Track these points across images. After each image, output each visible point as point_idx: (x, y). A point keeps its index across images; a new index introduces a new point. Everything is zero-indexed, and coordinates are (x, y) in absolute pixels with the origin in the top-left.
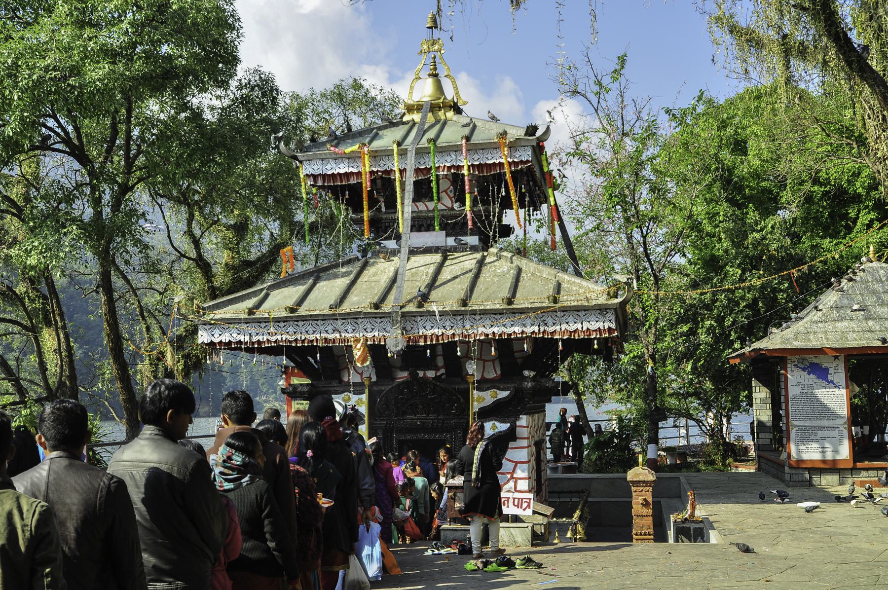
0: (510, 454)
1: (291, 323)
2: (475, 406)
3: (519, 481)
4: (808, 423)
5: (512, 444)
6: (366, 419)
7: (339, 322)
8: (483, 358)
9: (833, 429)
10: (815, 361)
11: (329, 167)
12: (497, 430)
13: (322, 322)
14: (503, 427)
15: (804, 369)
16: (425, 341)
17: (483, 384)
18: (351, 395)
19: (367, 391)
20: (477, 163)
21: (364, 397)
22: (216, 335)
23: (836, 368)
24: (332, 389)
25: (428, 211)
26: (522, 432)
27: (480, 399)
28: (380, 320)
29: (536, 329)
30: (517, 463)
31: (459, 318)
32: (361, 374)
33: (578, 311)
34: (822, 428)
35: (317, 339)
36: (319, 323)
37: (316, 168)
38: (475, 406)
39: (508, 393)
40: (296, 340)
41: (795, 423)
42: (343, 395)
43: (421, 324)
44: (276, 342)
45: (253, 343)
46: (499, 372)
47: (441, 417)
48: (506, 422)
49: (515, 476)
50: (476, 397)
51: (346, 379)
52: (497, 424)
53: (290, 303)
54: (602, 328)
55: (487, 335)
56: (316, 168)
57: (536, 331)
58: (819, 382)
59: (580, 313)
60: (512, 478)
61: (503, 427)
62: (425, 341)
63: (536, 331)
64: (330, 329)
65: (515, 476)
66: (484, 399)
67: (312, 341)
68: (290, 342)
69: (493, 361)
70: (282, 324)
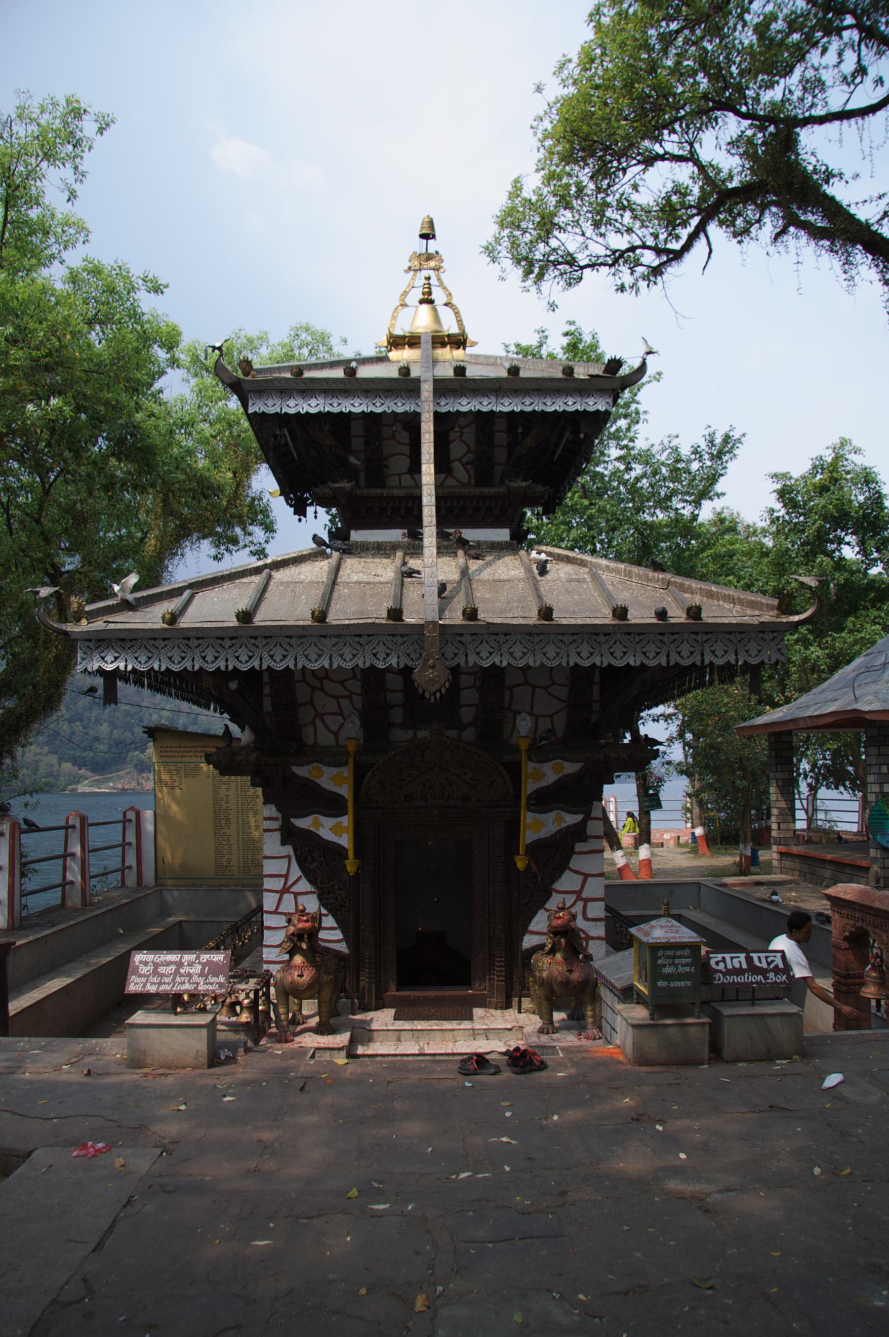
0: (576, 862)
2: (530, 786)
3: (590, 904)
5: (579, 847)
8: (535, 711)
11: (292, 403)
12: (564, 825)
17: (540, 751)
19: (351, 760)
21: (347, 772)
22: (109, 658)
30: (586, 876)
32: (336, 734)
33: (730, 633)
38: (530, 786)
39: (578, 766)
42: (310, 767)
49: (584, 895)
50: (530, 771)
51: (310, 741)
52: (563, 813)
53: (243, 604)
59: (732, 637)
60: (579, 898)
61: (571, 819)
65: (584, 895)
69: (551, 716)
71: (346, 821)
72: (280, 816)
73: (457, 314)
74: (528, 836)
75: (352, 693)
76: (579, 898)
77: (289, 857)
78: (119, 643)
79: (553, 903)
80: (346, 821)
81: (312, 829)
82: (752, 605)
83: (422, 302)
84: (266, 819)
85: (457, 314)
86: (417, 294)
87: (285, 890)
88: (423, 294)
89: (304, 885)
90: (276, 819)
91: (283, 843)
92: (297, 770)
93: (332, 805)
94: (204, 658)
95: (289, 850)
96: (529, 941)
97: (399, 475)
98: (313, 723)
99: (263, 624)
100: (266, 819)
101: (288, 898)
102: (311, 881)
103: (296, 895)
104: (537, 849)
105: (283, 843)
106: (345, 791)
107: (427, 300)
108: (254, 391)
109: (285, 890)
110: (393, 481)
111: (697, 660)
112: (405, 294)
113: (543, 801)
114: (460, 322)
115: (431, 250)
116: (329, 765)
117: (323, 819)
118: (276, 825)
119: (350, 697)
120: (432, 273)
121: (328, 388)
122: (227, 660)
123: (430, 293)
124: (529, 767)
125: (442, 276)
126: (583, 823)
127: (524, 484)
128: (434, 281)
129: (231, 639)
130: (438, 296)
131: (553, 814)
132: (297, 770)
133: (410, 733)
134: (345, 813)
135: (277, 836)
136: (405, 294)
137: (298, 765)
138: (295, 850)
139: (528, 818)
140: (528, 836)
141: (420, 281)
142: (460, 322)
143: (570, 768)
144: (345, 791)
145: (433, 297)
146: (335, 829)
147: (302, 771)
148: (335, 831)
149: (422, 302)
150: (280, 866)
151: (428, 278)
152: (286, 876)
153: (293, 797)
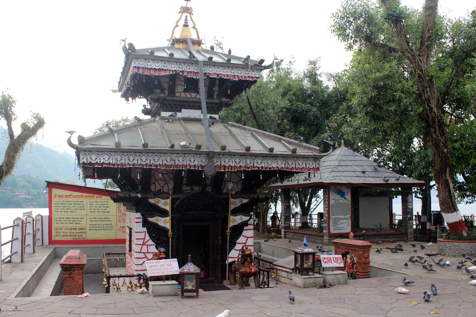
0: (244, 233)
1: (144, 154)
2: (232, 207)
4: (337, 217)
5: (246, 228)
6: (170, 213)
7: (175, 155)
9: (346, 219)
10: (340, 189)
11: (149, 64)
12: (243, 220)
13: (164, 155)
15: (336, 193)
16: (225, 169)
18: (160, 199)
19: (170, 197)
20: (233, 74)
21: (169, 201)
23: (348, 192)
24: (149, 196)
25: (192, 98)
27: (235, 203)
28: (199, 156)
29: (284, 166)
30: (248, 238)
31: (244, 157)
34: (341, 219)
35: (160, 164)
36: (162, 155)
37: (141, 63)
38: (232, 207)
40: (146, 165)
41: (332, 216)
42: (155, 199)
43: (222, 160)
44: (133, 165)
45: (118, 165)
46: (240, 189)
47: (210, 212)
48: (247, 216)
50: (232, 201)
52: (243, 217)
55: (259, 168)
56: (141, 63)
57: (284, 167)
58: (341, 198)
62: (225, 169)
63: (284, 167)
64: (169, 159)
66: (236, 203)
67: (156, 166)
68: (143, 165)
69: (237, 182)
70: (138, 154)
71: (168, 219)
72: (141, 217)
73: (197, 32)
74: (231, 224)
75: (168, 173)
76: (245, 245)
77: (145, 232)
78: (97, 153)
79: (238, 247)
80: (168, 219)
81: (156, 222)
82: (309, 148)
84: (136, 218)
85: (197, 32)
86: (182, 23)
87: (144, 244)
88: (185, 23)
89: (151, 242)
90: (140, 218)
91: (143, 226)
92: (150, 200)
93: (164, 213)
94: (129, 159)
95: (145, 229)
96: (230, 260)
97: (180, 93)
98: (155, 183)
99: (152, 148)
100: (136, 218)
101: (145, 247)
102: (153, 241)
103: (147, 245)
104: (234, 228)
105: (143, 226)
106: (168, 208)
107: (186, 25)
108: (136, 58)
109: (144, 244)
110: (177, 95)
111: (294, 166)
112: (178, 21)
113: (236, 212)
114: (198, 35)
115: (189, 6)
116: (162, 199)
117: (159, 218)
118: (141, 220)
119: (168, 174)
120: (188, 15)
121: (162, 59)
122: (138, 160)
123: (187, 23)
124: (232, 200)
125: (192, 16)
126: (249, 220)
127: (226, 100)
128: (189, 18)
129: (139, 153)
130: (190, 24)
131: (239, 217)
132: (150, 200)
133: (189, 188)
134: (168, 216)
135: (141, 224)
136: (178, 21)
137: (151, 198)
138: (147, 229)
139: (231, 218)
140: (231, 224)
141: (184, 17)
142: (198, 35)
143: (245, 201)
144: (168, 208)
145: (188, 24)
146: (164, 222)
147: (152, 201)
148: (165, 222)
149: (184, 26)
150: (142, 236)
151: (186, 17)
152: (144, 239)
153: (147, 210)
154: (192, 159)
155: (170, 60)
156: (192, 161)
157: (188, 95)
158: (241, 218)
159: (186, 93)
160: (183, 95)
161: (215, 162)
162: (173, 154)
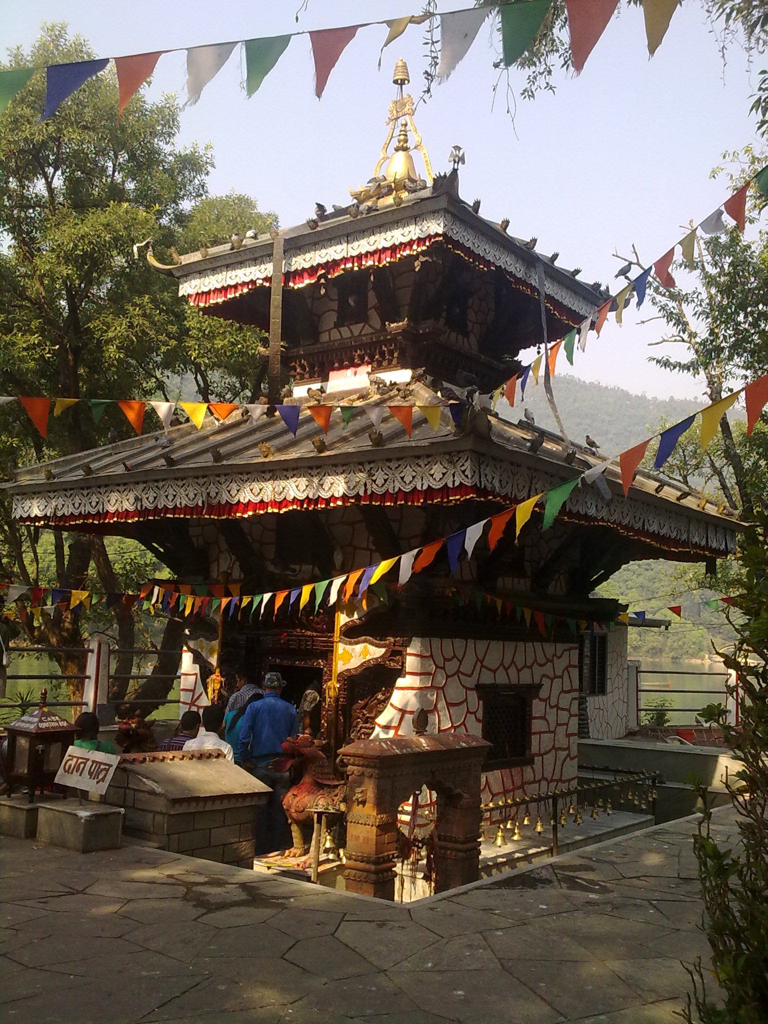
12: (368, 657)
14: (375, 652)
26: (411, 663)
54: (450, 486)
57: (362, 493)
61: (375, 652)
64: (132, 497)
77: (196, 674)
83: (397, 150)
86: (395, 143)
123: (406, 141)
139: (341, 648)
152: (193, 691)
154: (171, 491)
155: (240, 259)
156: (171, 498)
157: (345, 332)
158: (365, 652)
159: (342, 329)
160: (335, 335)
161: (213, 494)
162: (138, 483)
